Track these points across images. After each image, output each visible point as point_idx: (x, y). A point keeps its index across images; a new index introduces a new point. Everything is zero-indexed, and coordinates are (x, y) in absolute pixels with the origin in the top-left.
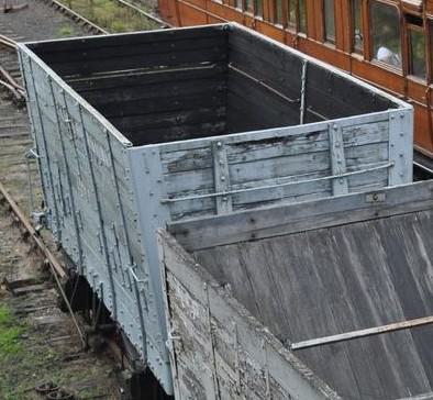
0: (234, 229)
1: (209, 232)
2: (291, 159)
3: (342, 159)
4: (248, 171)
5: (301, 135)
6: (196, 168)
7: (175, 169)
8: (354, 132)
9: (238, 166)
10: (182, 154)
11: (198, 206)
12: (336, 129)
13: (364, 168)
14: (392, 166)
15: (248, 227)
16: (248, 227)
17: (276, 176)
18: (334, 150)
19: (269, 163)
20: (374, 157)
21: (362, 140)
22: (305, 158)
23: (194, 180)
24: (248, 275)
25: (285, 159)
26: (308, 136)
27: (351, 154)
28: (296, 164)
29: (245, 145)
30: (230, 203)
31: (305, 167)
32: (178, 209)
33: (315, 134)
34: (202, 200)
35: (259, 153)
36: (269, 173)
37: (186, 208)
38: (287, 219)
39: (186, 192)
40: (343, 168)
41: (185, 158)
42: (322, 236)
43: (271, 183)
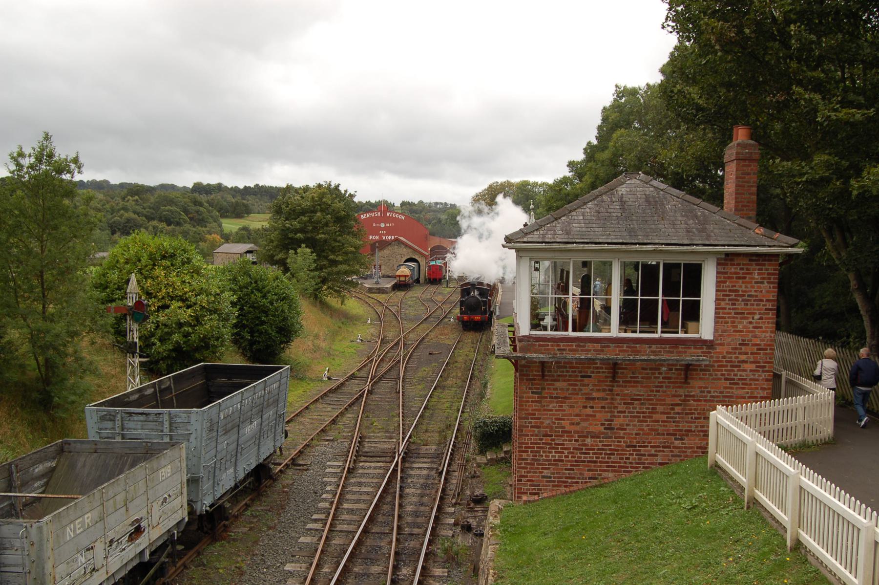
0: (88, 446)
1: (79, 446)
3: (168, 426)
4: (131, 425)
6: (111, 420)
7: (103, 419)
8: (176, 416)
13: (180, 432)
15: (94, 447)
16: (94, 447)
21: (179, 420)
23: (109, 424)
24: (84, 466)
28: (151, 425)
29: (130, 414)
31: (155, 427)
32: (102, 435)
35: (136, 418)
36: (139, 427)
37: (106, 435)
38: (110, 446)
39: (106, 429)
40: (168, 430)
42: (122, 456)
43: (140, 432)
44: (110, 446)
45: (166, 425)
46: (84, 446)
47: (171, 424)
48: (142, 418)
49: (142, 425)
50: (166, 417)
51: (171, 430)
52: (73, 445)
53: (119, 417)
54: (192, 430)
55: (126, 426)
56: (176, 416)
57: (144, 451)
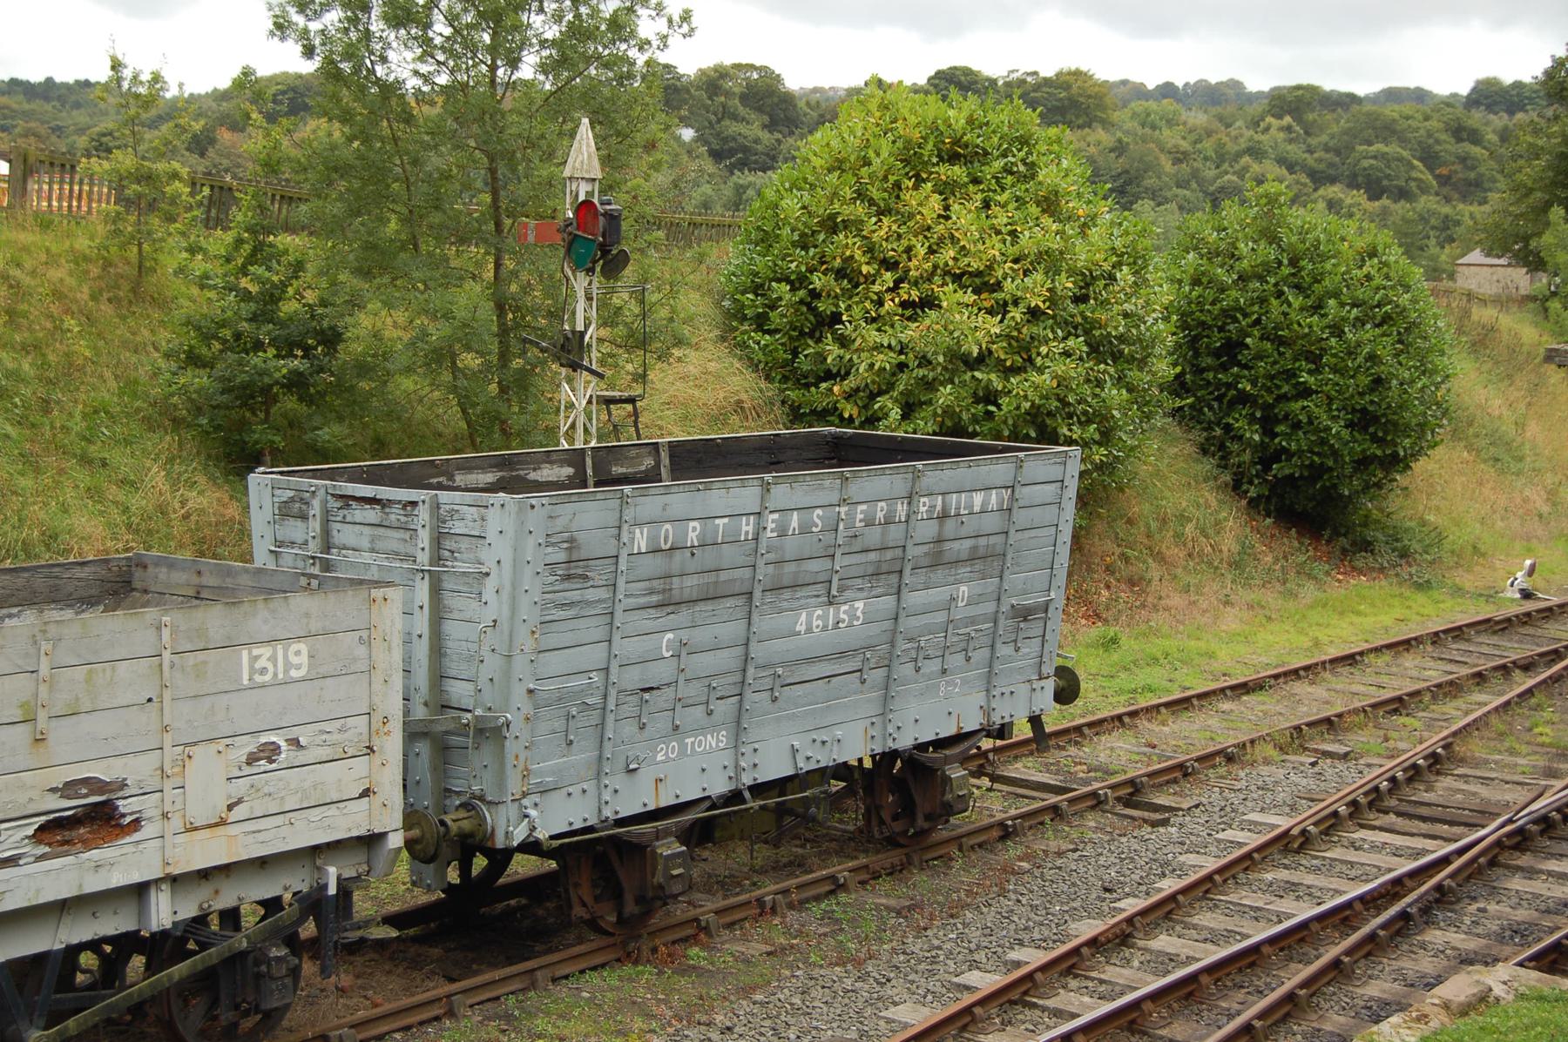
2: (389, 533)
5: (400, 502)
8: (452, 513)
13: (461, 567)
14: (487, 574)
17: (372, 550)
18: (420, 531)
19: (367, 530)
21: (459, 527)
25: (381, 531)
29: (347, 499)
36: (365, 544)
41: (292, 500)
43: (367, 558)
45: (424, 538)
47: (438, 539)
50: (423, 513)
51: (437, 559)
53: (316, 508)
55: (337, 538)
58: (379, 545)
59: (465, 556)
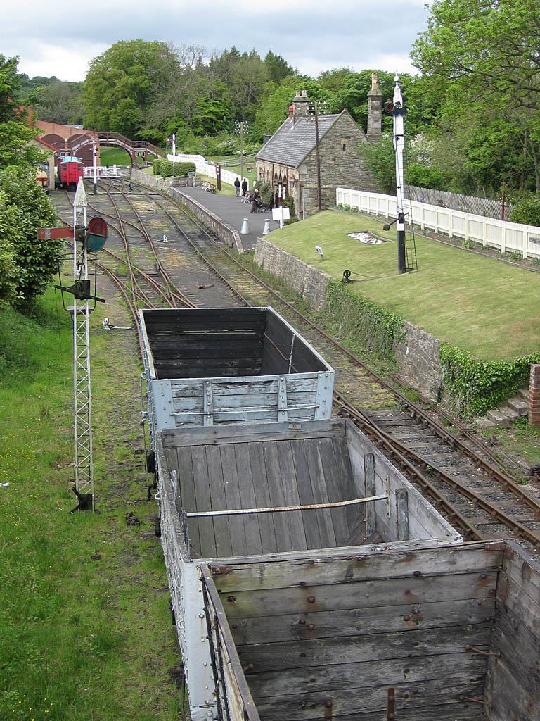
0: (203, 436)
1: (188, 436)
2: (253, 396)
4: (226, 401)
5: (260, 382)
7: (180, 396)
8: (295, 383)
9: (219, 398)
10: (186, 386)
11: (192, 419)
12: (282, 381)
13: (300, 406)
18: (280, 393)
19: (239, 397)
20: (307, 400)
22: (262, 396)
23: (192, 403)
25: (248, 396)
26: (265, 383)
27: (292, 397)
28: (257, 400)
29: (224, 385)
30: (212, 419)
31: (262, 402)
32: (180, 420)
33: (270, 382)
34: (195, 416)
35: (233, 390)
36: (238, 403)
37: (185, 420)
38: (237, 434)
40: (285, 405)
41: (186, 389)
43: (239, 410)
44: (237, 434)
45: (283, 396)
46: (197, 436)
48: (243, 390)
49: (242, 401)
50: (282, 386)
52: (177, 436)
54: (319, 402)
55: (218, 403)
56: (295, 383)
57: (289, 436)
58: (247, 403)
59: (303, 401)
